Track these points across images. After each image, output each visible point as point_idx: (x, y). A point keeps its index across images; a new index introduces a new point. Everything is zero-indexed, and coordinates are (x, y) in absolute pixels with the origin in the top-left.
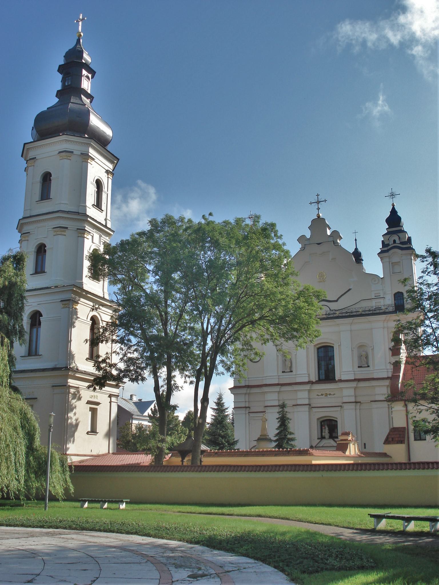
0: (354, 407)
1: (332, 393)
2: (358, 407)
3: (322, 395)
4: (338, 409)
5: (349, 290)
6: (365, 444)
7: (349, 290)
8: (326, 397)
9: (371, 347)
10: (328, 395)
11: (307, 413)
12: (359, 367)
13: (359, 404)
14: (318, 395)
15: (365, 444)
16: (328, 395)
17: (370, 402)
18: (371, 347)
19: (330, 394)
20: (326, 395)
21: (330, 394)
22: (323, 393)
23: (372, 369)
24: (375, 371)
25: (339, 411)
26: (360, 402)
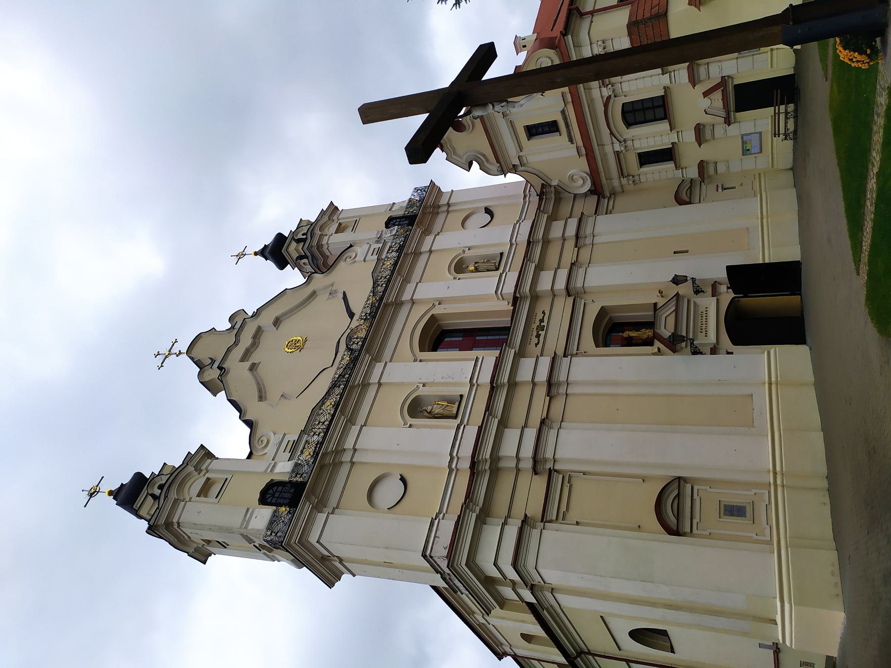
1: (540, 316)
3: (538, 336)
5: (345, 298)
7: (345, 298)
9: (464, 252)
10: (542, 324)
14: (536, 345)
18: (464, 252)
19: (542, 321)
21: (542, 321)
22: (535, 333)
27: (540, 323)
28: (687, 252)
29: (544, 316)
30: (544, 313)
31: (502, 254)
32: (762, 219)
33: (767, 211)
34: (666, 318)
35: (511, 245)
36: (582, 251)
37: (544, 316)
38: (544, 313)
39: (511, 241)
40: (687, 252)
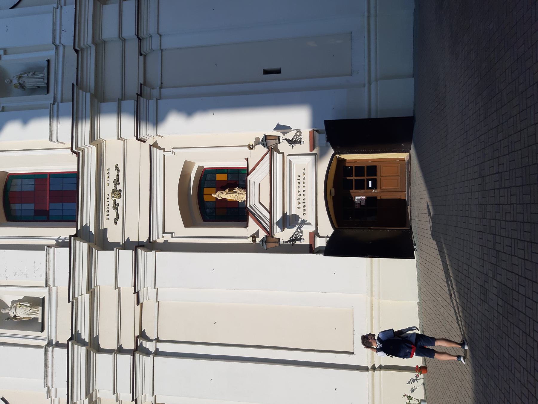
0: (152, 104)
2: (156, 92)
4: (158, 154)
6: (266, 72)
8: (122, 194)
10: (119, 187)
11: (159, 254)
12: (48, 92)
13: (145, 88)
15: (266, 72)
16: (119, 187)
17: (142, 58)
19: (116, 182)
20: (116, 193)
22: (112, 204)
23: (53, 52)
24: (57, 42)
25: (165, 154)
26: (141, 84)
27: (115, 187)
28: (278, 72)
29: (118, 176)
30: (117, 168)
31: (48, 61)
32: (369, 17)
33: (376, 7)
34: (260, 202)
35: (57, 47)
36: (149, 59)
37: (118, 176)
38: (117, 168)
39: (54, 43)
40: (278, 72)
